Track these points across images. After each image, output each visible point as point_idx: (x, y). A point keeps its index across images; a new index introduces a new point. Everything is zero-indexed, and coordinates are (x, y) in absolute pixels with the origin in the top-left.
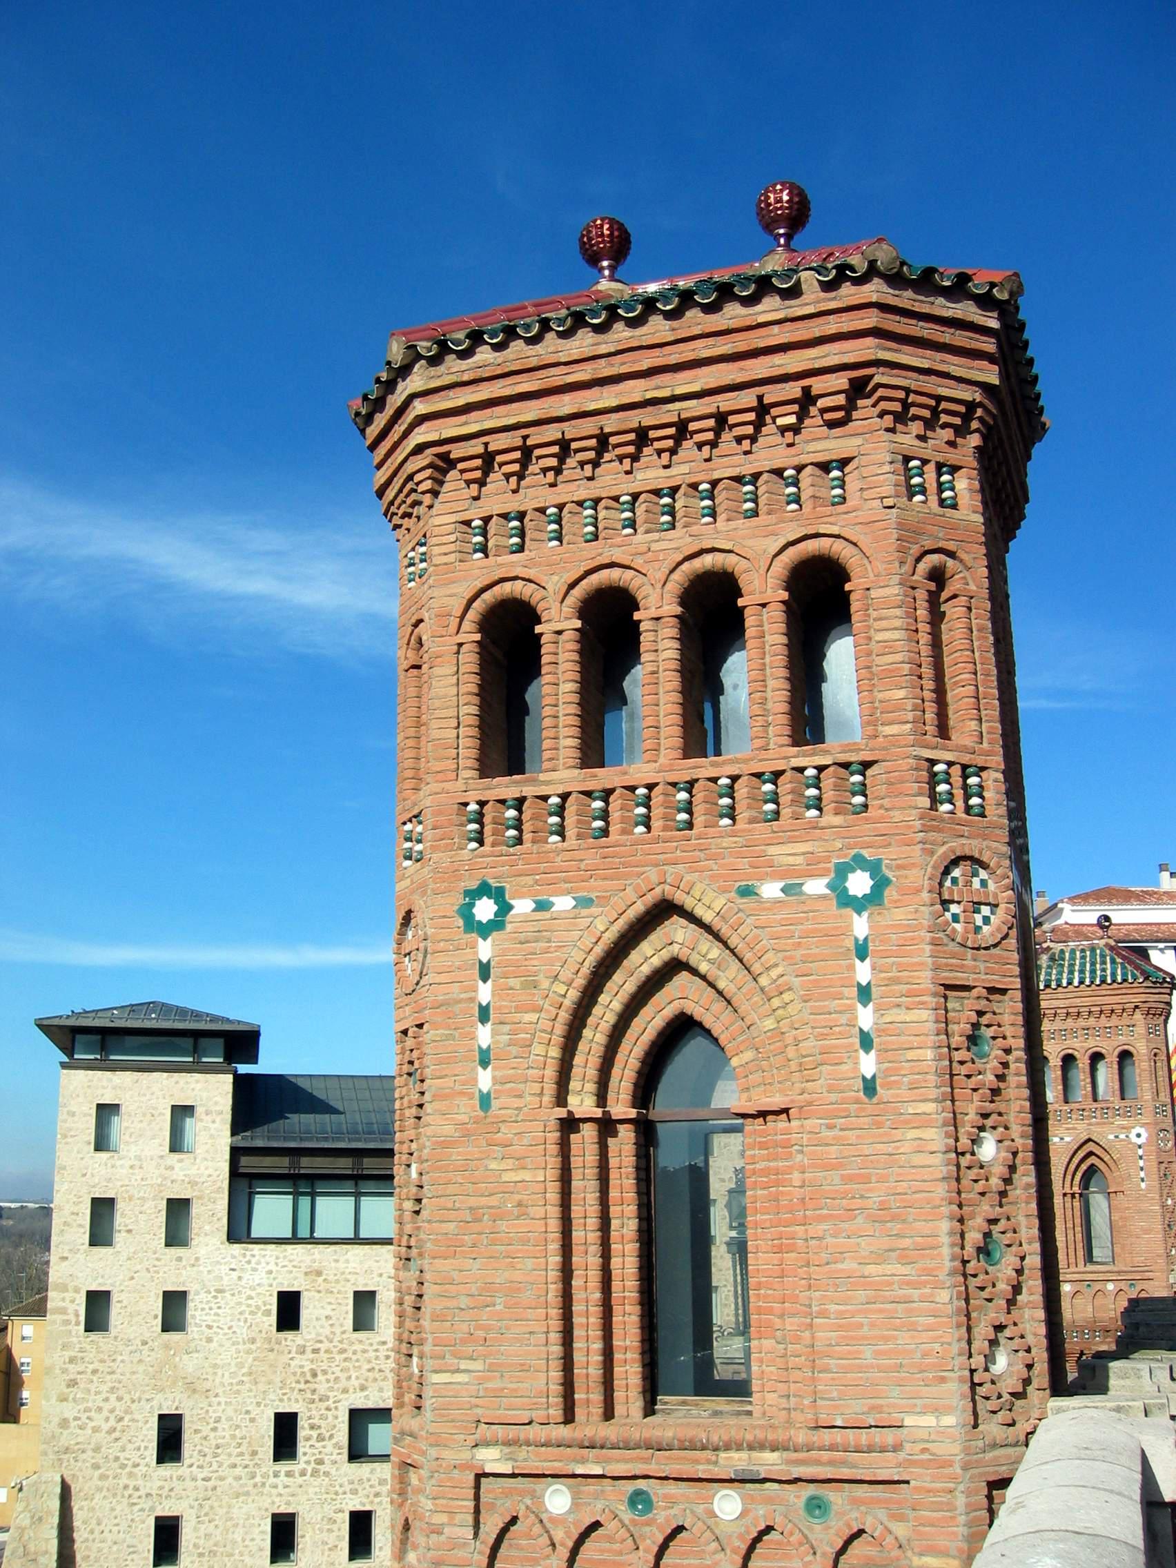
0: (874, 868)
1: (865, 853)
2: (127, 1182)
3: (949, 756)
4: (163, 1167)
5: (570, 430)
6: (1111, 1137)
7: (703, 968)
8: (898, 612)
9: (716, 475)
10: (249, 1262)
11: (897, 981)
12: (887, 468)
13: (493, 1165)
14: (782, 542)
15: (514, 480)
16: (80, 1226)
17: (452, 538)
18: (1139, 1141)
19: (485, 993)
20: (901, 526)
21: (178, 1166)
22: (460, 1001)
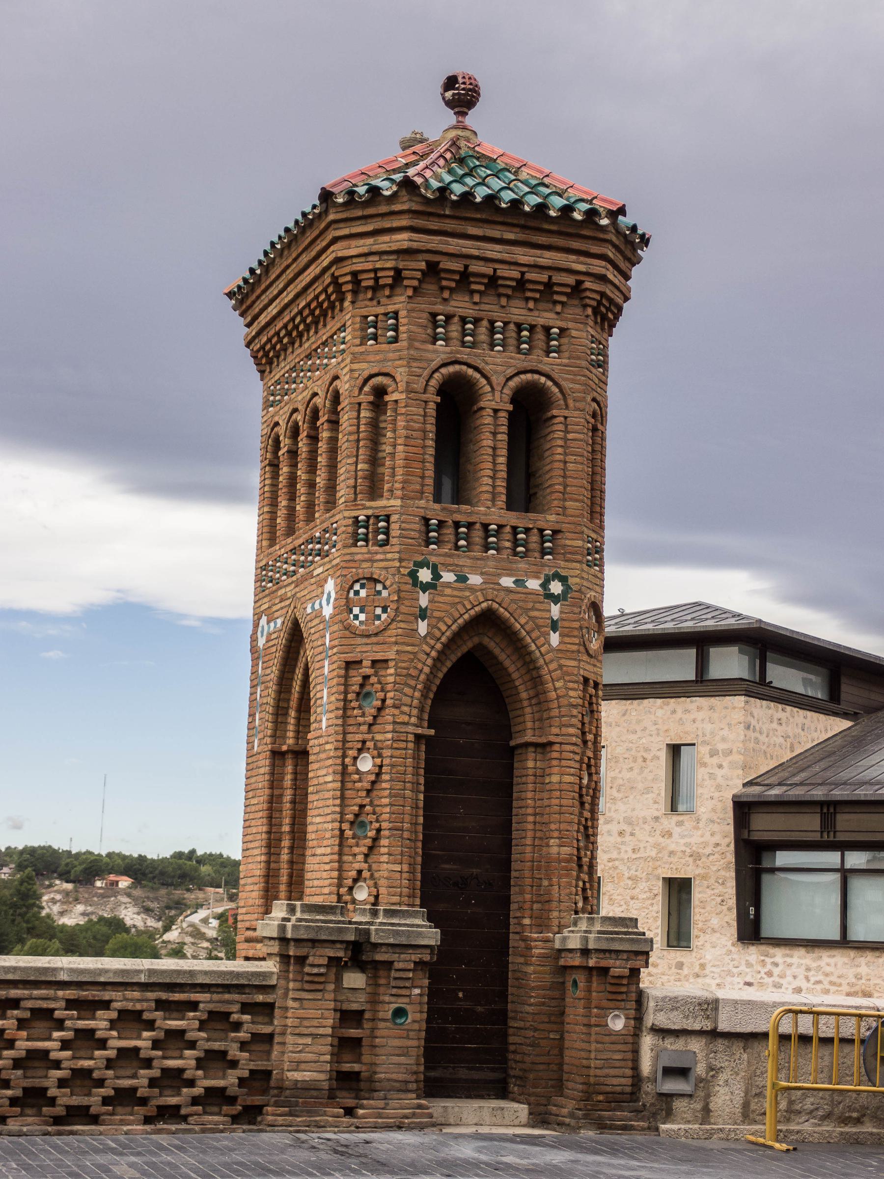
2: (614, 855)
4: (658, 832)
10: (770, 974)
21: (676, 831)
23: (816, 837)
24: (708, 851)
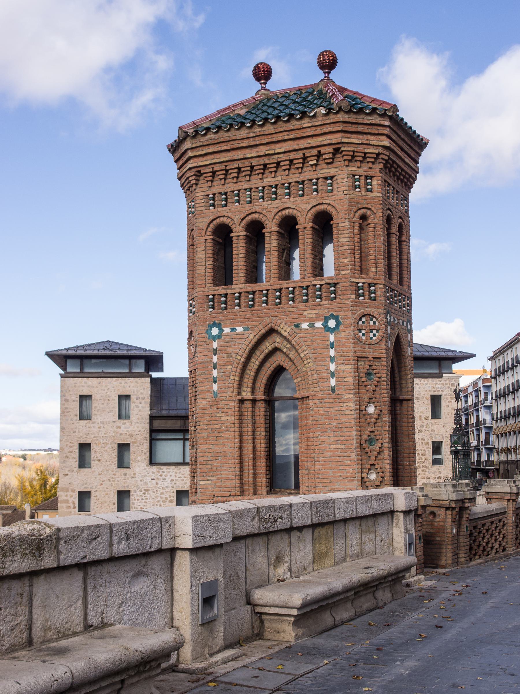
0: (336, 318)
1: (334, 314)
2: (96, 435)
3: (363, 281)
4: (115, 427)
5: (241, 164)
7: (285, 350)
8: (347, 232)
9: (290, 181)
10: (161, 475)
11: (342, 356)
12: (346, 180)
13: (218, 415)
14: (311, 206)
15: (223, 181)
16: (74, 458)
17: (203, 201)
19: (215, 359)
20: (349, 201)
21: (123, 426)
22: (207, 362)
23: (179, 428)
24: (136, 433)
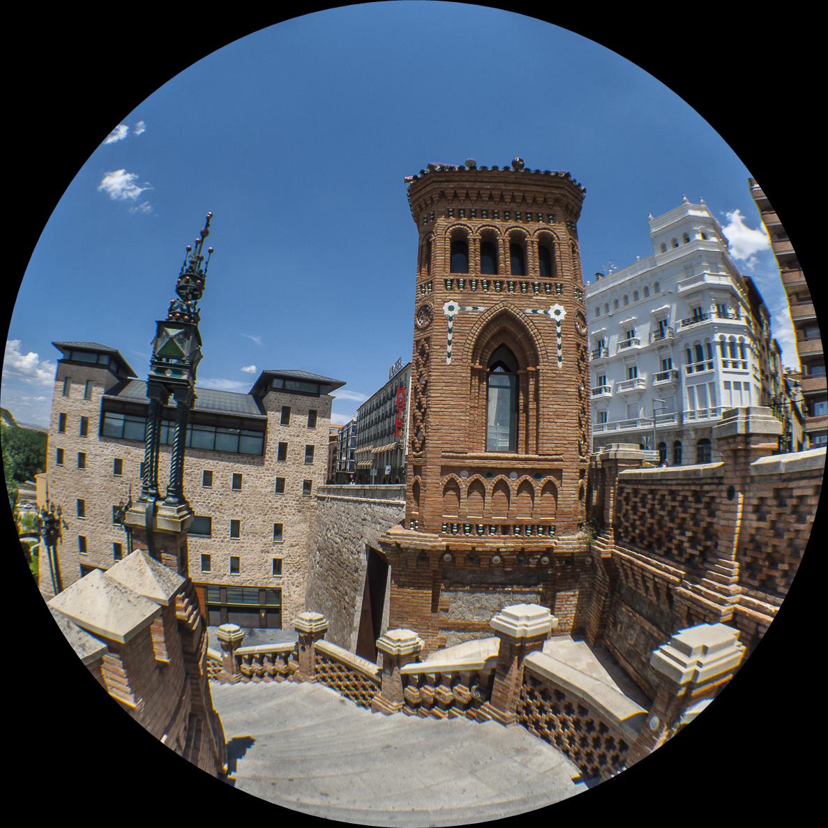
6: (529, 311)
18: (558, 318)
